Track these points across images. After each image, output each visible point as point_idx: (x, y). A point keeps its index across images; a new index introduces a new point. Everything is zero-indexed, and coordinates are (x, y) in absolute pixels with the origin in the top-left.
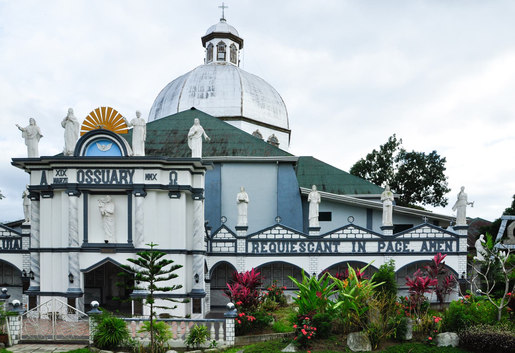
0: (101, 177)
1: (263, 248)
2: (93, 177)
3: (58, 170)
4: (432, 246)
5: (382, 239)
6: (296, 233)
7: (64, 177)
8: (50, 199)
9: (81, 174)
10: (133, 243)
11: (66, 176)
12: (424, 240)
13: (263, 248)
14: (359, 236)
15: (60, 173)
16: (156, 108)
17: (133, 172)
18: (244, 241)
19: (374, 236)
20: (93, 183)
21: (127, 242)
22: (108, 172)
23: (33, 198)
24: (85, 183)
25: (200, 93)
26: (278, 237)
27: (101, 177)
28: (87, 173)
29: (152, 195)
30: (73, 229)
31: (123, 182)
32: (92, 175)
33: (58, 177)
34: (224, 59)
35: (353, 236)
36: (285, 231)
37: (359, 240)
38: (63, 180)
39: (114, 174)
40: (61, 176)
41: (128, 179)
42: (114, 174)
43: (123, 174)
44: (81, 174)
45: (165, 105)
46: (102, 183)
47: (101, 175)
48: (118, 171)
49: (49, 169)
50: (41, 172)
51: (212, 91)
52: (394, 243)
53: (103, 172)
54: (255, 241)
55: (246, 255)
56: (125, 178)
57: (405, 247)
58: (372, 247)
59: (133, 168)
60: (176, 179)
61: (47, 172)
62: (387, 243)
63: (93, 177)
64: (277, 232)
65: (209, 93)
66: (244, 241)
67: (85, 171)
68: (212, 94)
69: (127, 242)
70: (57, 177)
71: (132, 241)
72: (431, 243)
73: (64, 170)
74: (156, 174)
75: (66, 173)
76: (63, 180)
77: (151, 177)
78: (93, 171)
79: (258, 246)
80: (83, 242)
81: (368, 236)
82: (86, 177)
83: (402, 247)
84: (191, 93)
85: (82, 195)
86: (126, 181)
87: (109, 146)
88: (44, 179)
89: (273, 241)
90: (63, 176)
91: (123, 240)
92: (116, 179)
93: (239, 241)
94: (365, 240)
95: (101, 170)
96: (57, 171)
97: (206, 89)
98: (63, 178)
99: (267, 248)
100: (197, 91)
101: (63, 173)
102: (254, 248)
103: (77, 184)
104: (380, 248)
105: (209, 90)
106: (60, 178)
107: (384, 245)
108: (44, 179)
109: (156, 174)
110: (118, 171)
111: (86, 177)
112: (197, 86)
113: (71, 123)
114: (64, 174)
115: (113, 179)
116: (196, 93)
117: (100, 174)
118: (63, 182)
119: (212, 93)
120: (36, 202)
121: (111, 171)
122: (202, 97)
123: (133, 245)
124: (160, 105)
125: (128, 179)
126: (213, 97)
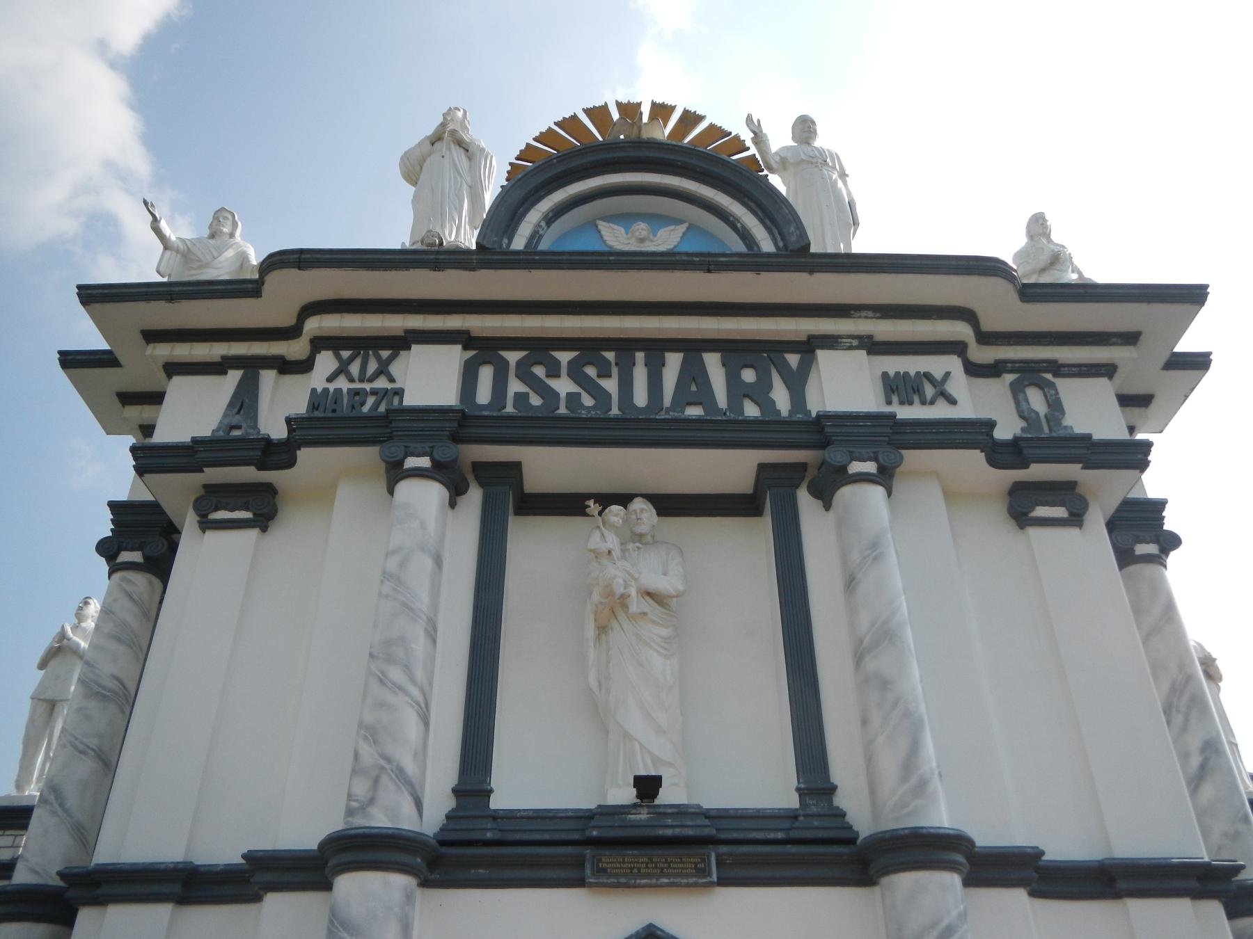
0: (610, 385)
2: (563, 386)
3: (346, 354)
7: (381, 383)
8: (252, 534)
9: (486, 375)
10: (842, 800)
11: (392, 380)
15: (355, 369)
21: (793, 802)
23: (125, 556)
27: (610, 385)
30: (401, 688)
31: (751, 410)
32: (558, 376)
33: (342, 384)
38: (371, 401)
39: (693, 374)
40: (361, 381)
42: (693, 374)
44: (486, 375)
47: (609, 376)
48: (713, 363)
49: (286, 367)
56: (760, 393)
61: (268, 377)
63: (563, 386)
67: (513, 357)
69: (793, 802)
70: (332, 387)
71: (832, 789)
73: (385, 354)
74: (947, 374)
75: (394, 369)
76: (371, 401)
77: (918, 390)
78: (564, 357)
80: (449, 803)
82: (515, 386)
85: (474, 497)
86: (766, 404)
88: (245, 401)
90: (371, 380)
95: (610, 356)
96: (338, 357)
98: (374, 392)
101: (372, 366)
103: (462, 411)
106: (356, 393)
108: (245, 401)
109: (947, 374)
110: (713, 363)
111: (515, 386)
113: (458, 154)
114: (383, 371)
115: (683, 396)
117: (605, 374)
118: (366, 409)
120: (141, 582)
121: (674, 361)
123: (842, 815)
125: (781, 397)
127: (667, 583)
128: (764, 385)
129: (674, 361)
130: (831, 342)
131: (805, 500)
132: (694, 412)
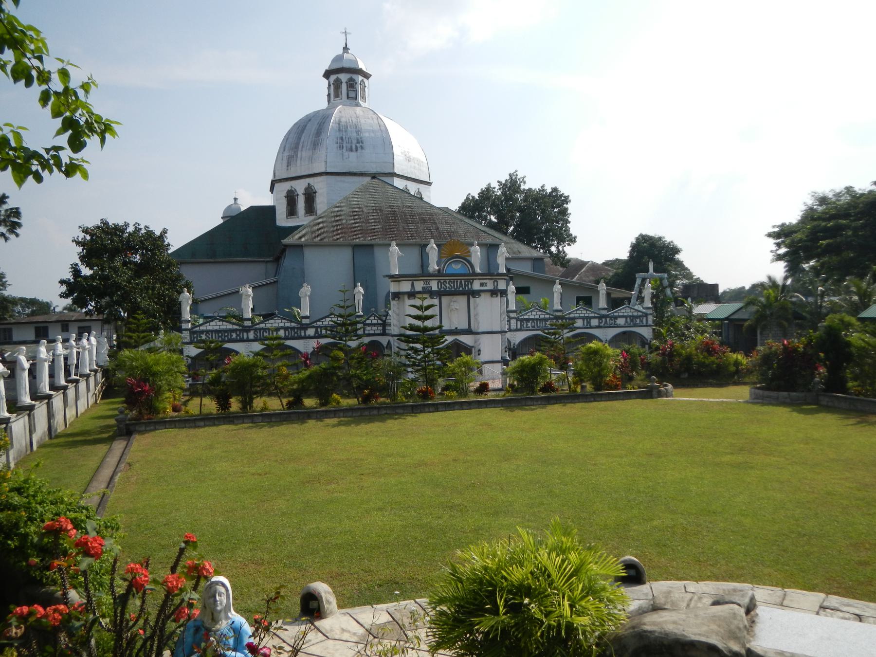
0: (452, 285)
1: (527, 325)
2: (448, 285)
4: (632, 321)
5: (601, 317)
6: (548, 314)
12: (626, 317)
13: (527, 325)
14: (587, 315)
16: (286, 154)
17: (473, 281)
18: (515, 321)
19: (596, 315)
20: (448, 289)
22: (457, 282)
24: (442, 289)
25: (349, 145)
26: (536, 317)
27: (452, 285)
28: (443, 282)
29: (483, 294)
34: (356, 98)
35: (582, 315)
36: (540, 313)
37: (587, 318)
39: (461, 283)
41: (470, 286)
42: (461, 283)
43: (467, 283)
45: (304, 154)
46: (453, 289)
48: (463, 281)
50: (411, 282)
51: (361, 144)
52: (608, 319)
53: (454, 282)
54: (522, 321)
55: (517, 330)
56: (468, 285)
57: (615, 322)
58: (595, 322)
59: (473, 279)
60: (497, 285)
62: (604, 320)
63: (448, 285)
64: (535, 313)
65: (358, 145)
66: (515, 321)
67: (442, 281)
68: (362, 147)
72: (630, 319)
78: (448, 281)
79: (524, 324)
81: (592, 315)
82: (443, 286)
83: (613, 322)
84: (338, 145)
86: (468, 288)
87: (460, 266)
89: (533, 320)
91: (464, 325)
92: (462, 286)
93: (511, 321)
94: (591, 318)
97: (354, 141)
99: (529, 325)
100: (345, 142)
102: (521, 325)
104: (600, 323)
105: (358, 143)
107: (602, 321)
111: (443, 286)
112: (344, 137)
115: (460, 287)
116: (344, 146)
119: (361, 147)
122: (351, 150)
124: (295, 152)
125: (470, 286)
126: (363, 151)
127: (457, 308)
128: (468, 284)
129: (459, 281)
130: (475, 279)
131: (471, 297)
132: (461, 289)
